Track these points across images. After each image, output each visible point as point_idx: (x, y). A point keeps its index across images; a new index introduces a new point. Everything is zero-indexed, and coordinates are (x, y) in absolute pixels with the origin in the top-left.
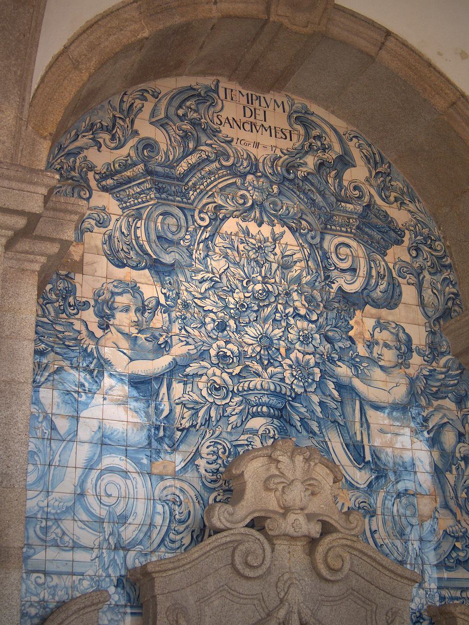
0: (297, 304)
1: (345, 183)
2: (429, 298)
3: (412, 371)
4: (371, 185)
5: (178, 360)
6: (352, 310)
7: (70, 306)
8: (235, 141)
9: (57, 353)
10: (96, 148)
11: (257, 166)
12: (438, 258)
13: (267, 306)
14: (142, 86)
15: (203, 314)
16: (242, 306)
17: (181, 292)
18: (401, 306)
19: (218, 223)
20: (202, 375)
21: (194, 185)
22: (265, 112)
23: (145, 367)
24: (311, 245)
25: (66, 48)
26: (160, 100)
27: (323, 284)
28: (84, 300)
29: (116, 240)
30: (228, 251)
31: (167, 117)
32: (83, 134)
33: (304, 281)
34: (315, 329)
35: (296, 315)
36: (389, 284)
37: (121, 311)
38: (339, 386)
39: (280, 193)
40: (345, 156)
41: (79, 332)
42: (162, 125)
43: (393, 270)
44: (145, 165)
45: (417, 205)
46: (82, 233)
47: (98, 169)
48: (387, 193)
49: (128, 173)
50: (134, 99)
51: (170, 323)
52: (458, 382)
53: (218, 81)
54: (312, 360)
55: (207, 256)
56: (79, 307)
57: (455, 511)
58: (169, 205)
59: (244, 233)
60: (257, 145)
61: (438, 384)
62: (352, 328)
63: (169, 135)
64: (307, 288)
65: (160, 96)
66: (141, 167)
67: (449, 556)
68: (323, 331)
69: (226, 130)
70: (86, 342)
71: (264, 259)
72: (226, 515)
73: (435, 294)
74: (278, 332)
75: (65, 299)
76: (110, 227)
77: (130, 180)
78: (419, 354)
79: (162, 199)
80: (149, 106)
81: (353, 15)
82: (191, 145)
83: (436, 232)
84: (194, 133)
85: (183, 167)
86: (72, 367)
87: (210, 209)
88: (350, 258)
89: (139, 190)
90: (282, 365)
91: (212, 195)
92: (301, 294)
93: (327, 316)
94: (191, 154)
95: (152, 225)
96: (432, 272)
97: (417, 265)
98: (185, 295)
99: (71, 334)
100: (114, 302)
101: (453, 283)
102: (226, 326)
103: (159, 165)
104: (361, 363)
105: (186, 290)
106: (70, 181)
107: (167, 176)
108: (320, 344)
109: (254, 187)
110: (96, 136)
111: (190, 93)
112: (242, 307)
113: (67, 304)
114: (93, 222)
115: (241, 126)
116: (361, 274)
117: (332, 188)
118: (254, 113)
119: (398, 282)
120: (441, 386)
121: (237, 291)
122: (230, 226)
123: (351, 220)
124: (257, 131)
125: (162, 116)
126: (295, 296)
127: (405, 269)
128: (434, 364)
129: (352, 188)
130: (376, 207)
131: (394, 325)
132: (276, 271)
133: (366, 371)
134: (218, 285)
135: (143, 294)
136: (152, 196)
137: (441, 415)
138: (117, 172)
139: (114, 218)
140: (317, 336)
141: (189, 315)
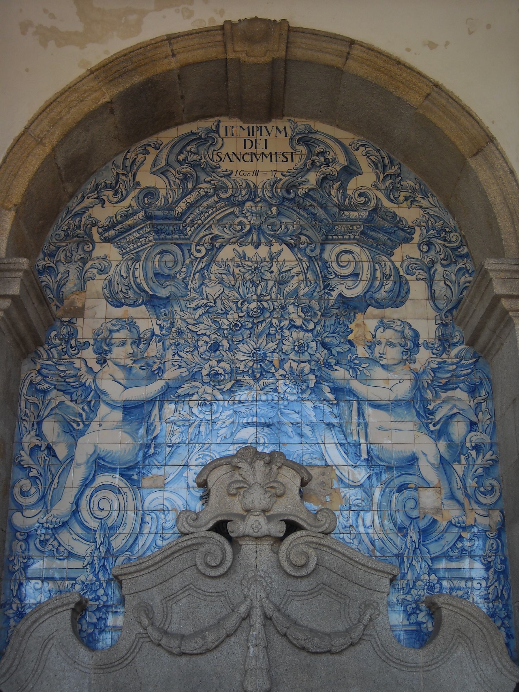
0: (293, 316)
1: (350, 192)
2: (441, 291)
3: (417, 366)
4: (378, 189)
5: (170, 383)
6: (352, 315)
7: (72, 348)
8: (234, 173)
9: (59, 390)
10: (100, 205)
11: (256, 193)
12: (452, 249)
13: (261, 322)
14: (145, 142)
15: (196, 338)
16: (236, 325)
17: (176, 321)
18: (408, 303)
19: (214, 252)
20: (194, 394)
21: (192, 221)
22: (266, 140)
24: (310, 258)
25: (26, 129)
26: (162, 150)
27: (323, 292)
28: (84, 340)
29: (116, 283)
30: (224, 276)
31: (168, 164)
32: (89, 195)
33: (301, 293)
34: (312, 338)
36: (395, 283)
37: (118, 346)
38: (336, 390)
39: (279, 213)
40: (350, 166)
41: (79, 369)
42: (163, 172)
43: (400, 269)
44: (145, 212)
45: (431, 200)
46: (85, 282)
47: (101, 224)
48: (396, 194)
49: (130, 222)
50: (136, 155)
51: (164, 350)
52: (472, 371)
53: (219, 121)
55: (203, 284)
56: (80, 348)
57: (462, 501)
58: (167, 244)
59: (240, 257)
60: (256, 173)
61: (449, 375)
62: (352, 331)
63: (169, 181)
64: (305, 301)
65: (161, 147)
66: (141, 215)
67: (454, 547)
68: (319, 338)
69: (226, 165)
70: (86, 377)
71: (260, 278)
72: (190, 520)
73: (448, 285)
74: (272, 345)
75: (67, 342)
76: (111, 273)
77: (131, 227)
79: (160, 239)
80: (150, 159)
82: (190, 186)
84: (194, 173)
85: (183, 205)
86: (72, 401)
87: (207, 240)
88: (353, 264)
89: (138, 235)
90: (274, 376)
91: (210, 227)
92: (298, 306)
93: (325, 323)
94: (190, 193)
95: (150, 264)
96: (445, 264)
97: (428, 259)
98: (179, 324)
99: (72, 372)
100: (111, 338)
101: (470, 271)
102: (219, 346)
103: (159, 209)
104: (360, 364)
105: (181, 319)
106: (75, 239)
107: (165, 218)
108: (316, 351)
109: (252, 213)
110: (101, 194)
112: (235, 327)
113: (69, 346)
114: (95, 271)
115: (241, 158)
116: (364, 277)
117: (335, 199)
118: (254, 144)
119: (406, 279)
120: (451, 377)
121: (231, 312)
123: (355, 227)
124: (258, 160)
125: (163, 164)
126: (291, 309)
127: (414, 265)
128: (444, 356)
129: (356, 195)
130: (383, 209)
131: (399, 323)
132: (272, 287)
133: (364, 370)
134: (212, 310)
135: (139, 328)
136: (151, 238)
137: (450, 406)
138: (119, 223)
139: (114, 264)
140: (314, 344)
141: (182, 341)
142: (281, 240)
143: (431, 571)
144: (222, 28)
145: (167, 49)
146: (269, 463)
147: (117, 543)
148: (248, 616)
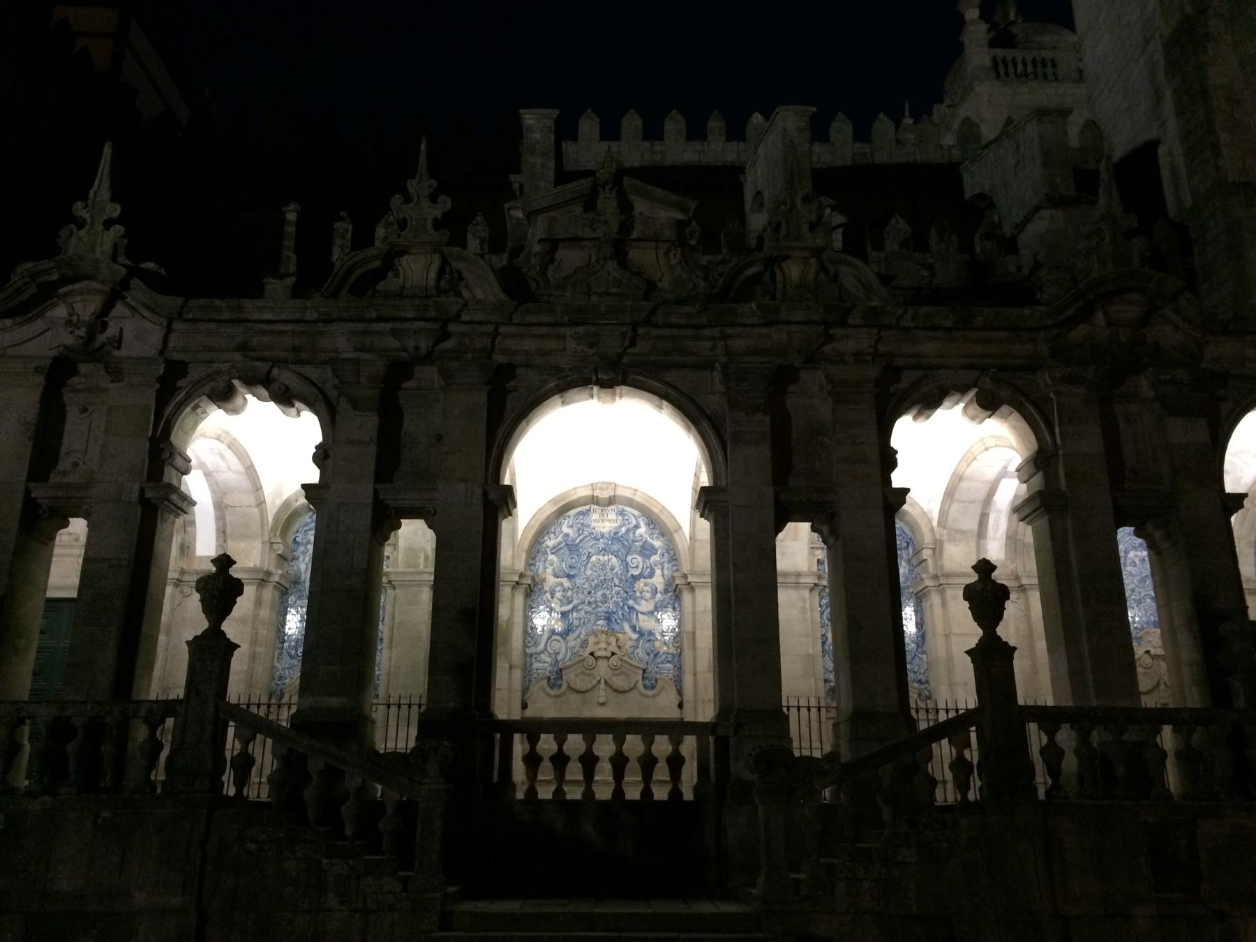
1: (636, 535)
18: (655, 577)
23: (565, 609)
24: (622, 561)
25: (528, 523)
35: (615, 585)
38: (629, 608)
39: (612, 543)
42: (571, 527)
49: (560, 546)
54: (620, 600)
64: (620, 576)
66: (564, 544)
67: (664, 660)
69: (593, 524)
78: (661, 593)
81: (624, 487)
82: (581, 533)
83: (671, 547)
85: (578, 541)
98: (577, 584)
107: (572, 545)
111: (581, 513)
112: (597, 585)
118: (603, 515)
122: (593, 559)
126: (615, 579)
142: (612, 554)
143: (657, 667)
144: (592, 484)
145: (573, 492)
146: (606, 635)
147: (559, 658)
148: (599, 681)
